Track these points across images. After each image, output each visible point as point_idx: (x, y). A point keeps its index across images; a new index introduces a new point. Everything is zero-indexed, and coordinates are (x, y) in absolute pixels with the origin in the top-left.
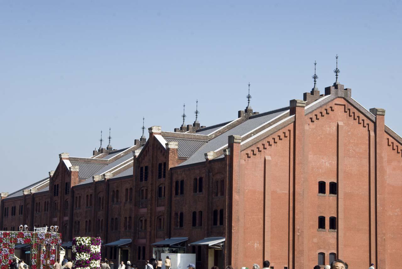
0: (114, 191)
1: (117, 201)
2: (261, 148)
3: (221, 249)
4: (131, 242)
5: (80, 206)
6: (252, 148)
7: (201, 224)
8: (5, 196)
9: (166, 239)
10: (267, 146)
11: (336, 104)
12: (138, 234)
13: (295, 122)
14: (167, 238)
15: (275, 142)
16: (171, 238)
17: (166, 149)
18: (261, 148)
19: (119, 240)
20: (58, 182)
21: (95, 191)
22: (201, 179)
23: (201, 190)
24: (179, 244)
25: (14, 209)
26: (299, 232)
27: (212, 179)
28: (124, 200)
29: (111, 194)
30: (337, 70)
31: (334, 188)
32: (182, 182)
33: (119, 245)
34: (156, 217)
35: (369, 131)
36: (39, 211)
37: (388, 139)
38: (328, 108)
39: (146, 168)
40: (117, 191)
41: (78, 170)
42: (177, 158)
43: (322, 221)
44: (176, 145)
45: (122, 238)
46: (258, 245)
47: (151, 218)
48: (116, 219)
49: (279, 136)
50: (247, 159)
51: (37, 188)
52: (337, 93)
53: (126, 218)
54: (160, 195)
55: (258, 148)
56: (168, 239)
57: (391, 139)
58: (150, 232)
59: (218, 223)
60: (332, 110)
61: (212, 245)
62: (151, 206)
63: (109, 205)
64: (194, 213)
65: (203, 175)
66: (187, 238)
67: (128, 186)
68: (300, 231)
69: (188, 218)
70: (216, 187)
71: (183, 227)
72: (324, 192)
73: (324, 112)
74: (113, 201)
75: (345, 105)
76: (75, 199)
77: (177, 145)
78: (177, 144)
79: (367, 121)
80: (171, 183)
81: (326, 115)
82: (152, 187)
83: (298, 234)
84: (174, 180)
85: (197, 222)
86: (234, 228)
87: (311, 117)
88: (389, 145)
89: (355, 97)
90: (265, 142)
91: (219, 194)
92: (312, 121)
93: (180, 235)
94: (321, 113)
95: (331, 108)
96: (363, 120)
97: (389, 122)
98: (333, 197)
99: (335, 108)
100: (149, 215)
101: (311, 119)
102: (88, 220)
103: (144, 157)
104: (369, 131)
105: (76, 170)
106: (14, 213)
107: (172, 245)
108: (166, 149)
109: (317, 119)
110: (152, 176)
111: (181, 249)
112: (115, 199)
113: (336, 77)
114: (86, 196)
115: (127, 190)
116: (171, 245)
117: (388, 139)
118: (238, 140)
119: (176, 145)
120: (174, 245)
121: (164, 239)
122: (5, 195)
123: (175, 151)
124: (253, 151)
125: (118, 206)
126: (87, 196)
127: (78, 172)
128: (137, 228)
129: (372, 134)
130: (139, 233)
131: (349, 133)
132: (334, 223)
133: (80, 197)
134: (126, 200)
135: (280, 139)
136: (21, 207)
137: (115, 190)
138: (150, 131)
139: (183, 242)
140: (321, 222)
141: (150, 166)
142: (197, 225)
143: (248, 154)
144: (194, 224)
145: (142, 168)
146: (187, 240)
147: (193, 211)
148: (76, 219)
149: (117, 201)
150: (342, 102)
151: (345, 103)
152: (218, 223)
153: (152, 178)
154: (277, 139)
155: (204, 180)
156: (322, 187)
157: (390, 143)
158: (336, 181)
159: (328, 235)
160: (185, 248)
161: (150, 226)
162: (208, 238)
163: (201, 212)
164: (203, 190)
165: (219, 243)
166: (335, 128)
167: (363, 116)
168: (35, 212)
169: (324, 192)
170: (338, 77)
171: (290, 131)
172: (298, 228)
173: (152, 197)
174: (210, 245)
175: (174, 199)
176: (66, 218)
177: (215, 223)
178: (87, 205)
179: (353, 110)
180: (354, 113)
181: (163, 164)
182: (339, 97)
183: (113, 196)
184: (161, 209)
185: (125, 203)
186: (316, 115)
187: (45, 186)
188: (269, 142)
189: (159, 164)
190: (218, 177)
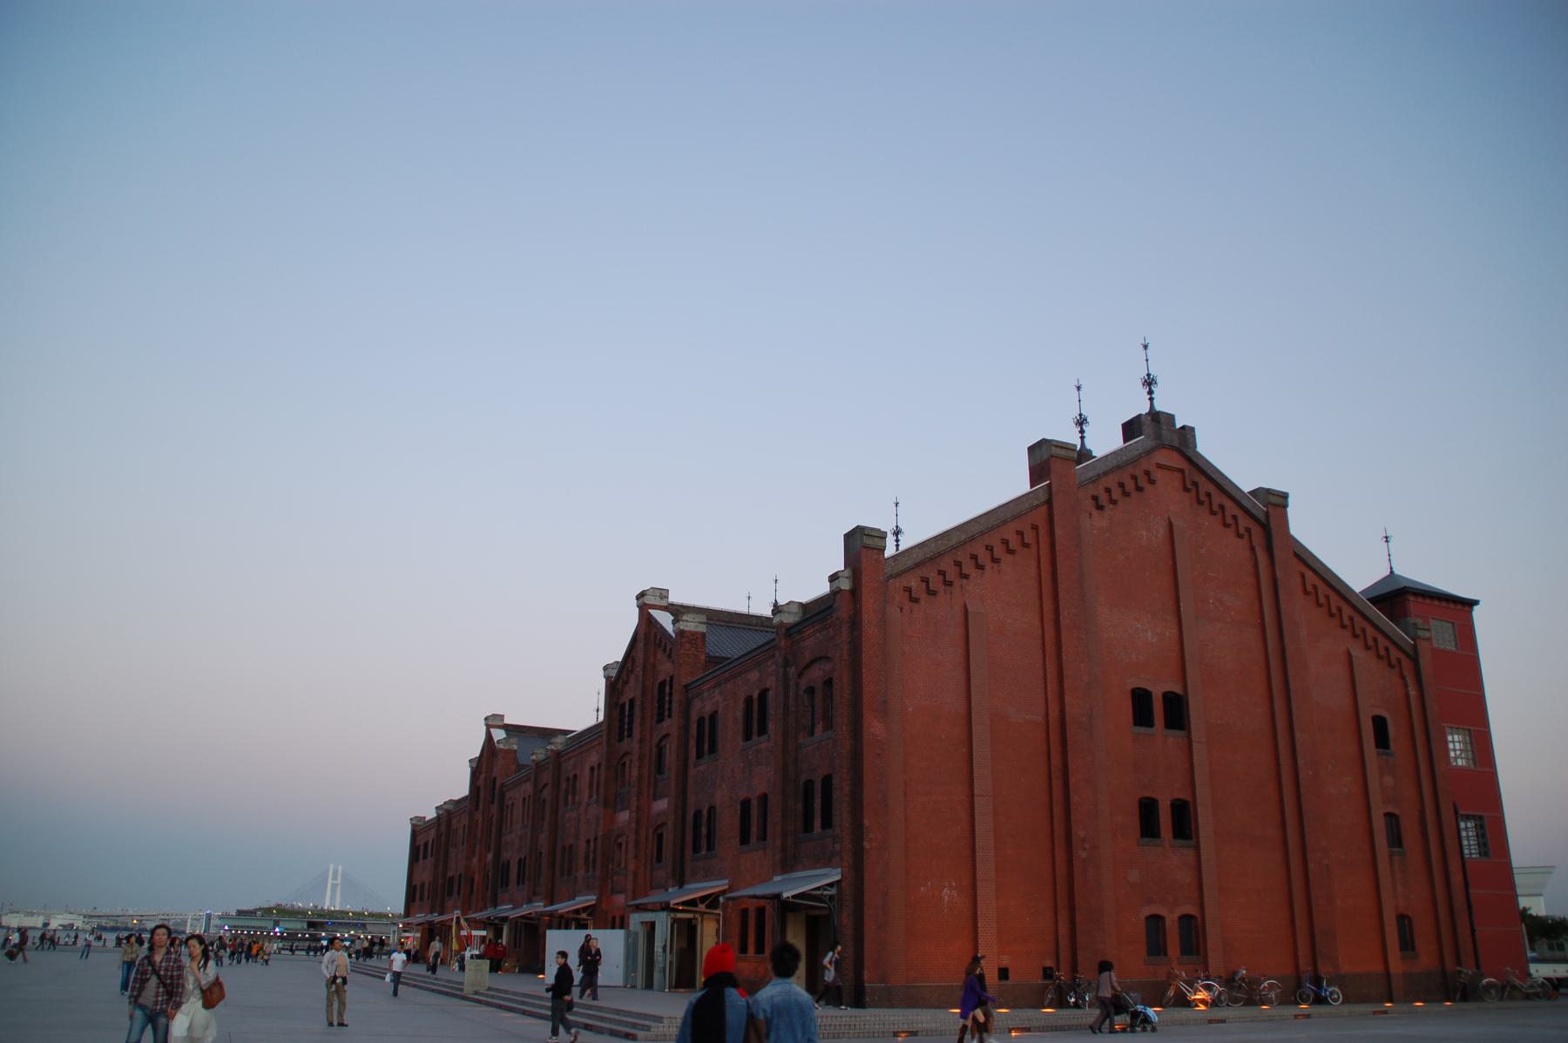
0: (568, 779)
1: (574, 802)
2: (952, 574)
3: (827, 912)
6: (924, 572)
7: (763, 837)
8: (419, 823)
9: (670, 890)
11: (1159, 466)
12: (612, 881)
13: (1049, 502)
14: (673, 886)
15: (995, 560)
16: (686, 887)
17: (673, 635)
18: (952, 574)
19: (574, 899)
21: (535, 786)
22: (763, 694)
23: (763, 730)
24: (702, 903)
26: (1085, 849)
27: (797, 685)
29: (564, 786)
30: (1149, 378)
31: (1176, 711)
32: (714, 716)
33: (560, 912)
34: (651, 830)
35: (1252, 549)
37: (1303, 576)
38: (1139, 473)
40: (575, 776)
41: (515, 747)
42: (703, 657)
43: (1147, 809)
44: (700, 623)
46: (955, 893)
47: (637, 833)
48: (571, 846)
49: (1005, 542)
50: (907, 605)
52: (1158, 436)
53: (588, 842)
54: (660, 770)
55: (942, 573)
56: (676, 888)
57: (1309, 574)
58: (635, 874)
59: (817, 822)
60: (1152, 482)
61: (793, 897)
62: (638, 800)
64: (746, 804)
65: (770, 682)
66: (727, 881)
67: (594, 758)
68: (1087, 846)
69: (728, 822)
70: (810, 709)
71: (714, 852)
72: (1150, 724)
73: (1130, 485)
75: (1182, 471)
77: (704, 623)
78: (705, 620)
79: (1244, 522)
80: (685, 728)
81: (1134, 494)
82: (640, 748)
83: (1084, 855)
84: (694, 717)
85: (754, 829)
86: (871, 836)
87: (1096, 494)
88: (1306, 592)
89: (1207, 447)
90: (962, 556)
91: (819, 727)
92: (1100, 508)
93: (708, 875)
94: (1121, 485)
95: (1147, 473)
96: (1234, 517)
98: (1174, 736)
99: (1159, 475)
100: (634, 825)
101: (1095, 498)
103: (628, 676)
104: (1252, 549)
105: (510, 747)
107: (678, 904)
108: (674, 636)
109: (1114, 502)
110: (643, 718)
111: (706, 916)
112: (570, 798)
113: (1149, 397)
114: (521, 799)
115: (592, 769)
116: (672, 902)
117: (1303, 576)
118: (876, 539)
119: (700, 623)
120: (683, 903)
121: (667, 890)
122: (420, 821)
123: (697, 638)
124: (925, 580)
126: (524, 799)
127: (515, 751)
128: (610, 866)
129: (1262, 557)
130: (615, 878)
131: (1203, 551)
133: (512, 804)
134: (590, 796)
135: (1010, 552)
137: (571, 776)
138: (641, 601)
139: (713, 894)
142: (753, 839)
143: (909, 590)
144: (744, 840)
146: (726, 887)
147: (742, 799)
148: (506, 855)
149: (574, 802)
150: (1174, 460)
151: (1183, 465)
152: (817, 822)
154: (999, 551)
155: (771, 694)
157: (1309, 588)
158: (1178, 690)
159: (1169, 856)
160: (719, 915)
161: (636, 857)
162: (786, 876)
163: (764, 798)
164: (771, 726)
165: (818, 889)
166: (1162, 532)
167: (1234, 506)
169: (1150, 724)
170: (1153, 396)
171: (1035, 528)
172: (1082, 834)
173: (640, 777)
174: (785, 895)
175: (692, 772)
176: (490, 856)
177: (808, 826)
178: (523, 822)
179: (1205, 486)
180: (1208, 495)
181: (668, 679)
182: (1164, 446)
183: (567, 790)
184: (662, 805)
185: (588, 805)
186: (1108, 490)
187: (460, 787)
188: (974, 557)
189: (660, 683)
190: (816, 673)
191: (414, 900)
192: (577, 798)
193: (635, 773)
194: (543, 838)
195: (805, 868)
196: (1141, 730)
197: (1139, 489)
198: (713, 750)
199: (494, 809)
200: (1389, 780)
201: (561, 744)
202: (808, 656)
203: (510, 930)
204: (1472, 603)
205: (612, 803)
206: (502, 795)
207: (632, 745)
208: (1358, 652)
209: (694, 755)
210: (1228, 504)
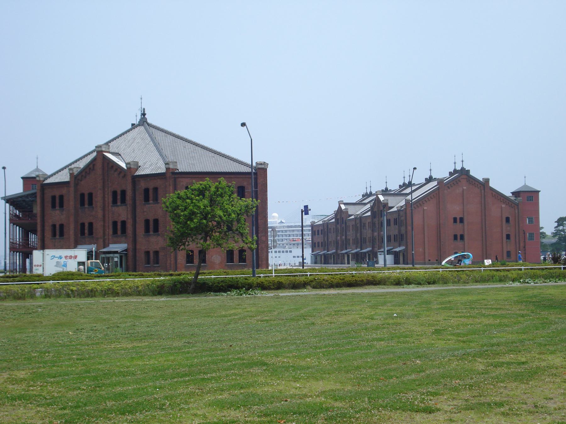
10: (424, 202)
11: (462, 178)
20: (339, 217)
25: (318, 231)
31: (462, 220)
37: (492, 193)
74: (363, 228)
97: (492, 184)
98: (461, 224)
106: (318, 234)
110: (378, 216)
132: (462, 237)
134: (369, 228)
136: (322, 230)
140: (455, 237)
141: (377, 211)
150: (465, 177)
153: (378, 218)
156: (455, 220)
163: (397, 235)
171: (436, 194)
191: (315, 246)
193: (377, 226)
194: (359, 235)
196: (454, 224)
197: (457, 183)
198: (390, 225)
199: (344, 225)
200: (509, 228)
204: (539, 191)
205: (373, 231)
206: (346, 223)
207: (376, 220)
208: (503, 206)
210: (476, 183)
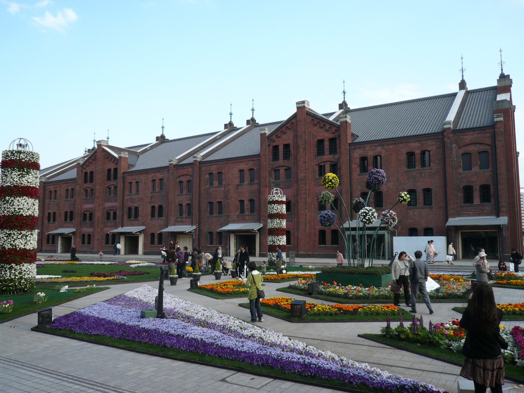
4: (262, 226)
5: (138, 191)
28: (237, 181)
36: (55, 198)
39: (287, 146)
40: (219, 173)
45: (234, 222)
48: (220, 203)
51: (47, 177)
53: (242, 202)
63: (202, 188)
76: (127, 185)
102: (157, 206)
125: (222, 189)
126: (154, 181)
145: (276, 148)
149: (220, 183)
168: (47, 201)
178: (154, 189)
192: (224, 182)
195: (469, 215)
201: (200, 158)
202: (467, 142)
203: (145, 237)
209: (358, 170)
